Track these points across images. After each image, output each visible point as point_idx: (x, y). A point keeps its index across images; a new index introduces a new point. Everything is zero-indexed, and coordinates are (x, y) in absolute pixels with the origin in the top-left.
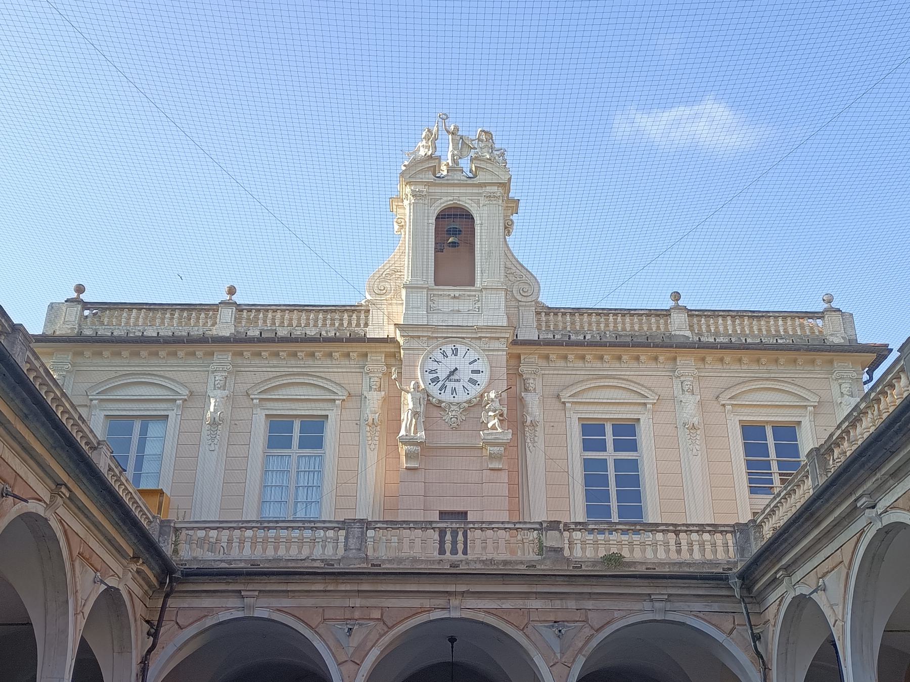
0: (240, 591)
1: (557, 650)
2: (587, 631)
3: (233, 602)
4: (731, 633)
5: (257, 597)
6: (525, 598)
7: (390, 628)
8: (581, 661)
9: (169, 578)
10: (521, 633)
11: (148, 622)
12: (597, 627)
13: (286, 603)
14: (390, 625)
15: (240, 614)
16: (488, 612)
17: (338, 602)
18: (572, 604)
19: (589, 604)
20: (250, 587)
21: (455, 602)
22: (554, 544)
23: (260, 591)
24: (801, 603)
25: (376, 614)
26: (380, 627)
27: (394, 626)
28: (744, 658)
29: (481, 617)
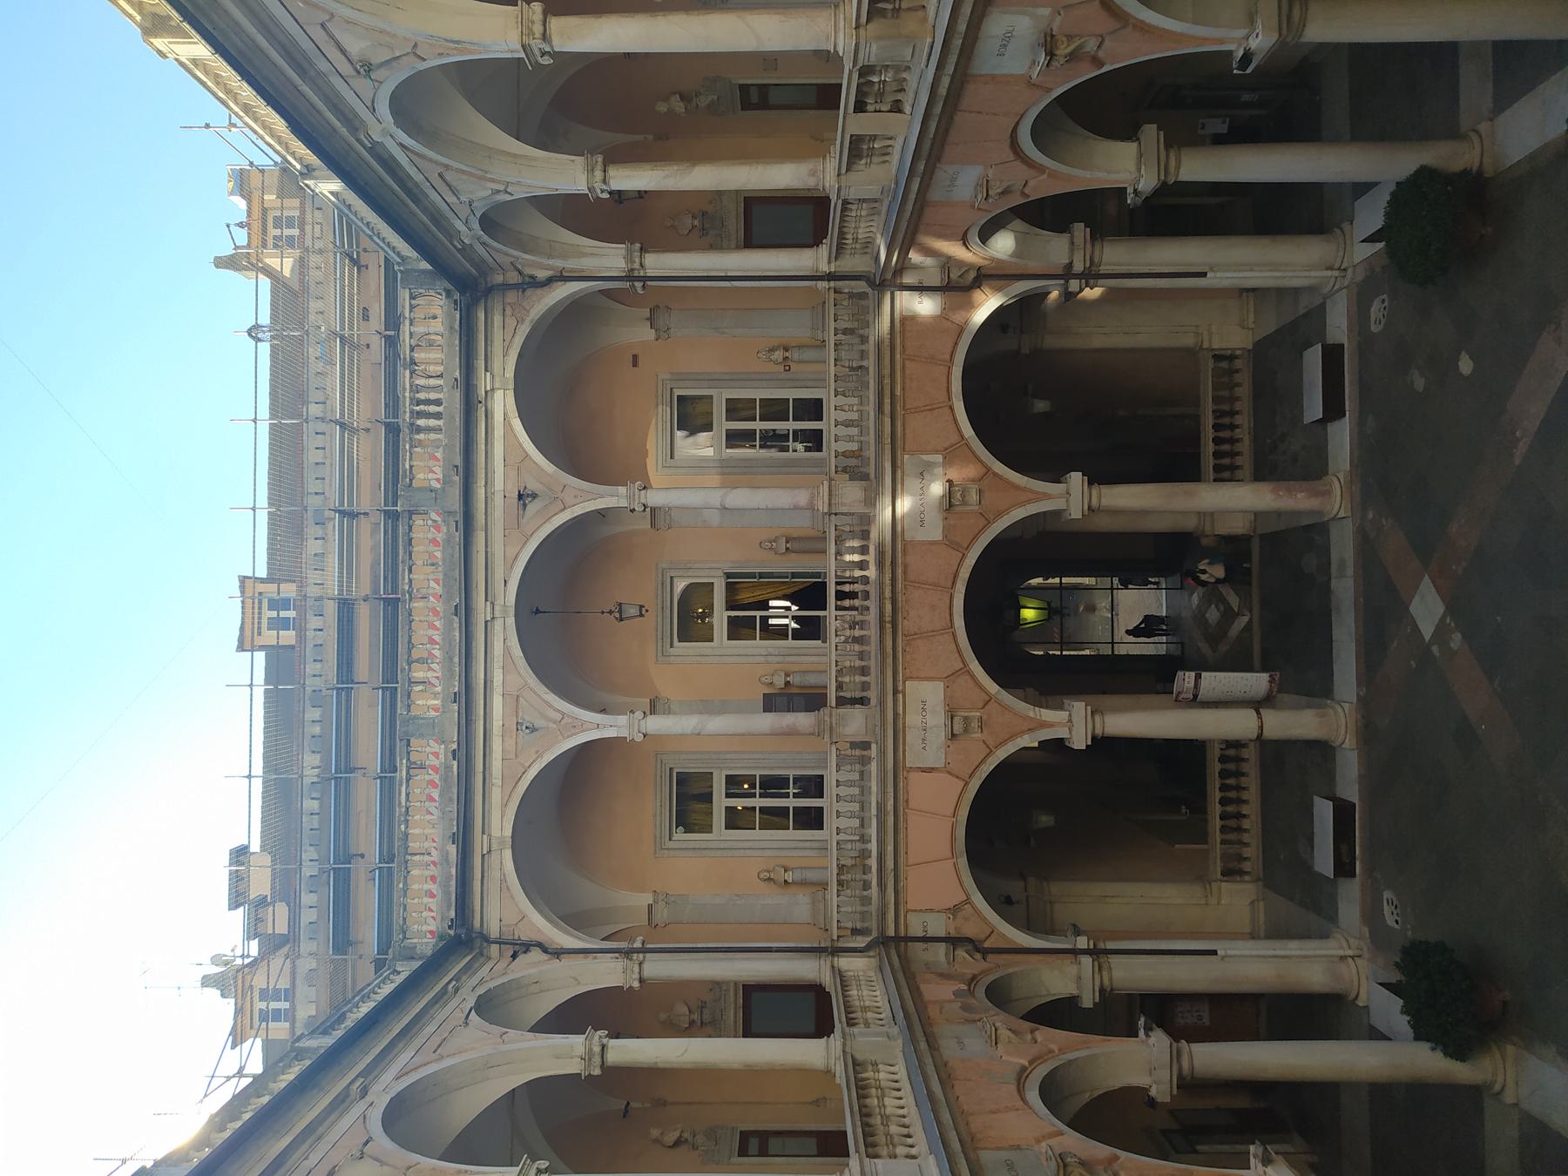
9: (464, 938)
11: (514, 956)
24: (489, 223)
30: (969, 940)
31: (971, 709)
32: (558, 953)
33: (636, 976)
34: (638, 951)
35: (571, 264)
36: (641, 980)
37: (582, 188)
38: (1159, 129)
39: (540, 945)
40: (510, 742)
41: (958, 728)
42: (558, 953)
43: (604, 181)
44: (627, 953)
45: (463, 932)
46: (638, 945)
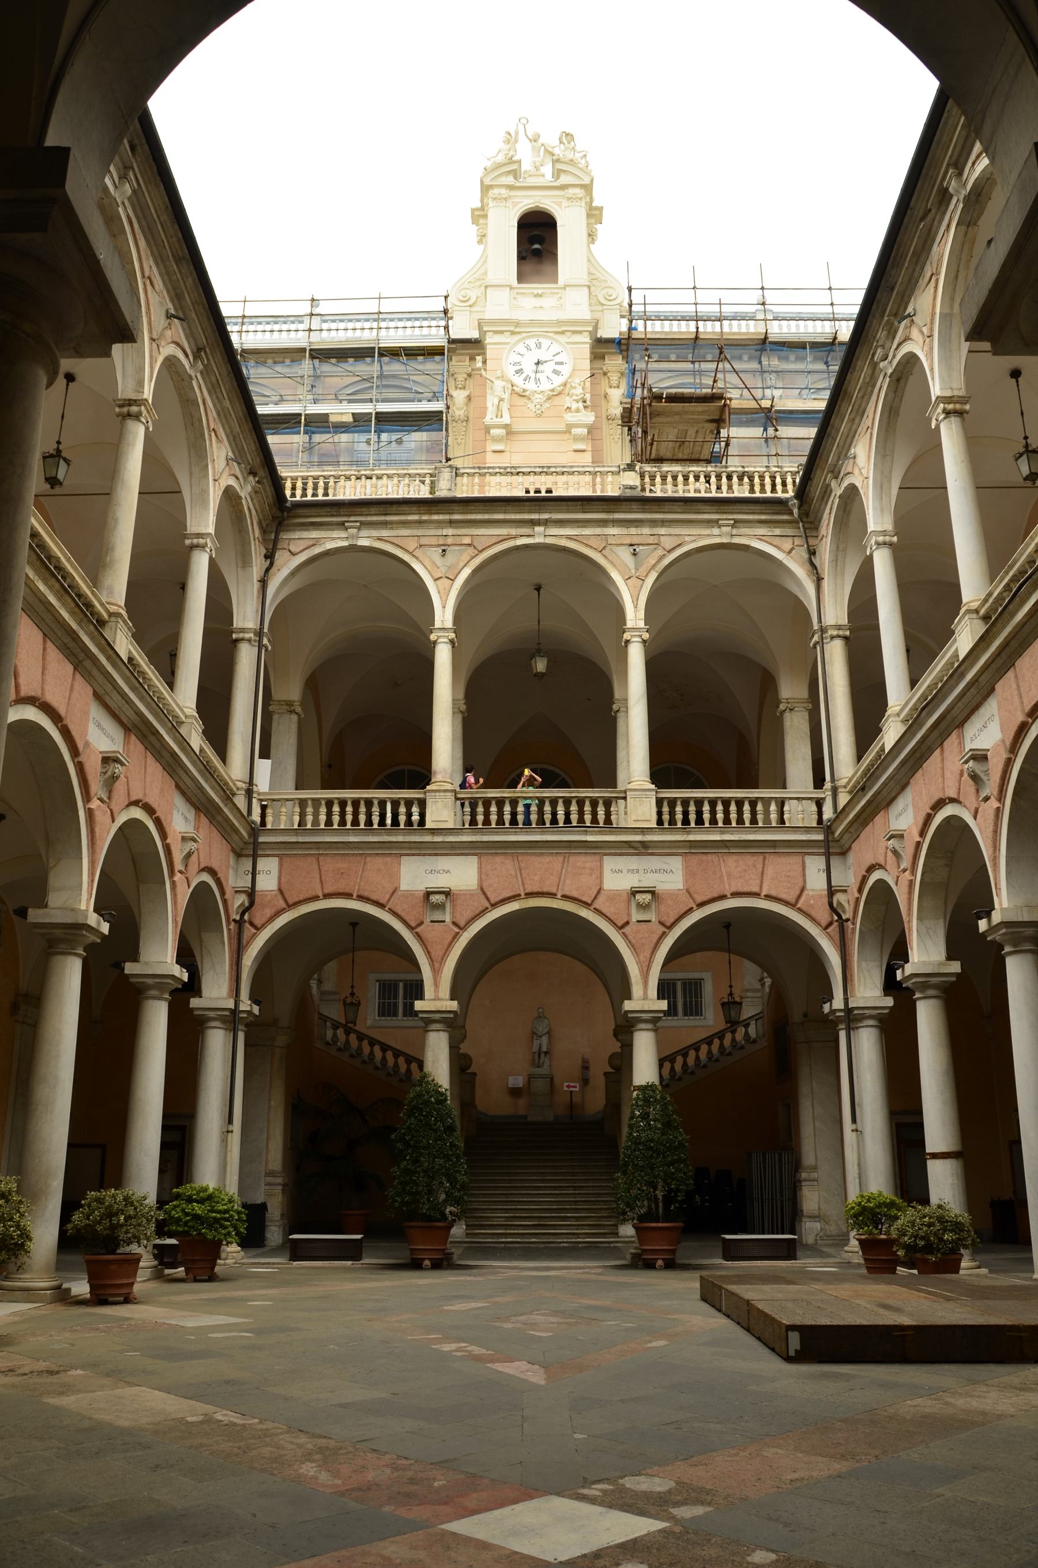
0: (343, 523)
1: (632, 566)
2: (660, 552)
3: (335, 534)
4: (790, 552)
5: (359, 529)
6: (603, 526)
7: (481, 552)
8: (653, 576)
10: (599, 555)
12: (669, 548)
13: (384, 533)
14: (480, 548)
15: (345, 544)
16: (569, 538)
17: (432, 532)
18: (646, 531)
19: (662, 531)
20: (352, 519)
21: (539, 529)
22: (631, 483)
23: (362, 523)
25: (467, 540)
26: (471, 551)
27: (484, 550)
28: (800, 571)
29: (564, 542)
30: (252, 903)
31: (453, 913)
32: (264, 582)
33: (241, 635)
34: (260, 642)
35: (826, 584)
36: (237, 641)
37: (871, 527)
38: (957, 975)
39: (272, 564)
40: (434, 541)
41: (434, 898)
42: (264, 582)
43: (878, 544)
44: (260, 633)
45: (288, 505)
46: (265, 641)
